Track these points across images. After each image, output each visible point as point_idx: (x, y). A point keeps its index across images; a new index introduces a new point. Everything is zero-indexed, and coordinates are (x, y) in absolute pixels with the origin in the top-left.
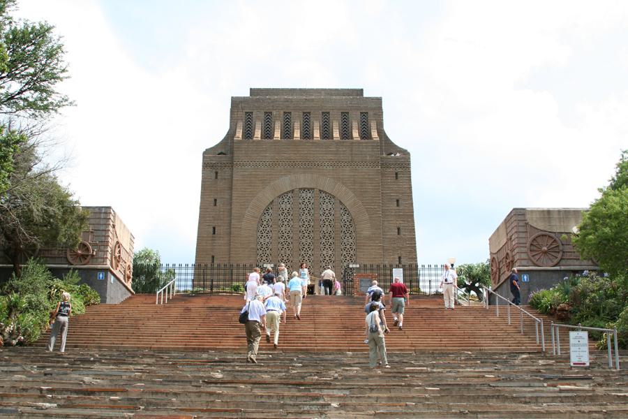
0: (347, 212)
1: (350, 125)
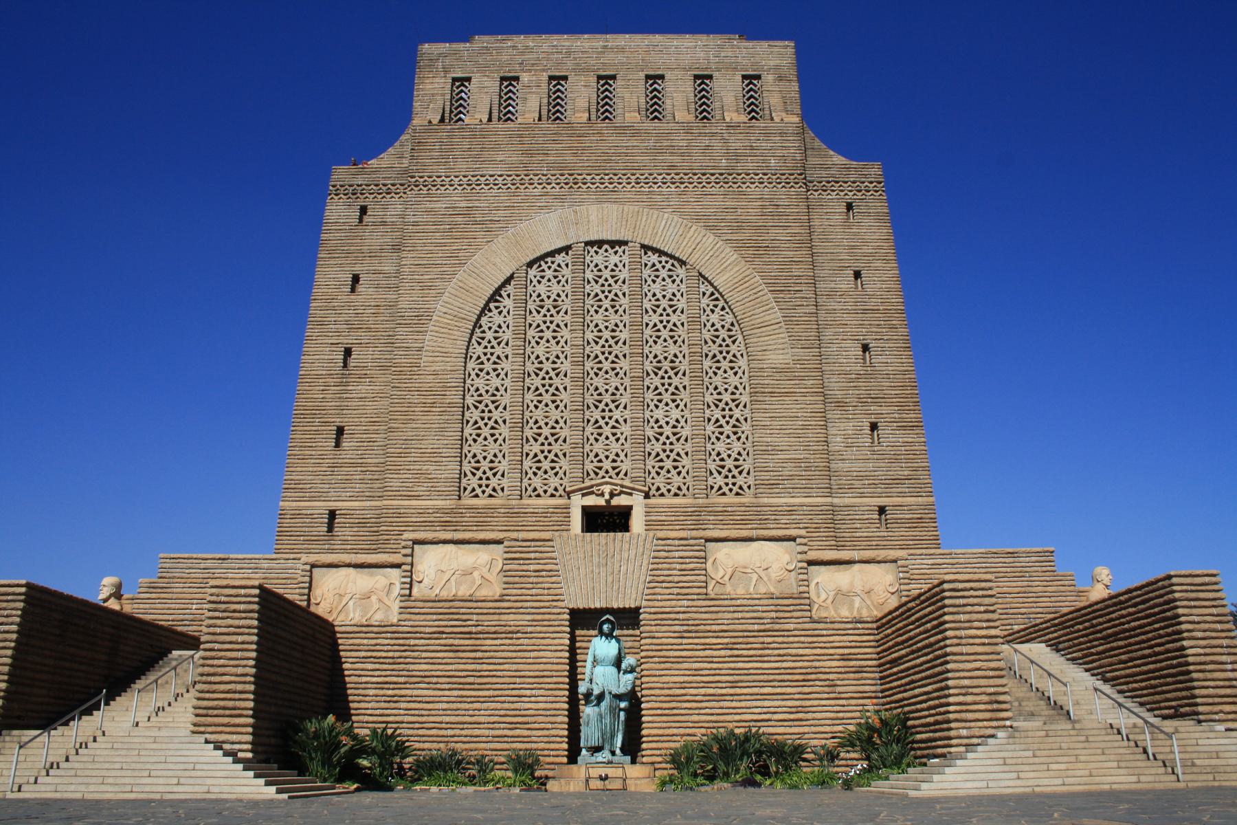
0: (721, 303)
1: (717, 105)
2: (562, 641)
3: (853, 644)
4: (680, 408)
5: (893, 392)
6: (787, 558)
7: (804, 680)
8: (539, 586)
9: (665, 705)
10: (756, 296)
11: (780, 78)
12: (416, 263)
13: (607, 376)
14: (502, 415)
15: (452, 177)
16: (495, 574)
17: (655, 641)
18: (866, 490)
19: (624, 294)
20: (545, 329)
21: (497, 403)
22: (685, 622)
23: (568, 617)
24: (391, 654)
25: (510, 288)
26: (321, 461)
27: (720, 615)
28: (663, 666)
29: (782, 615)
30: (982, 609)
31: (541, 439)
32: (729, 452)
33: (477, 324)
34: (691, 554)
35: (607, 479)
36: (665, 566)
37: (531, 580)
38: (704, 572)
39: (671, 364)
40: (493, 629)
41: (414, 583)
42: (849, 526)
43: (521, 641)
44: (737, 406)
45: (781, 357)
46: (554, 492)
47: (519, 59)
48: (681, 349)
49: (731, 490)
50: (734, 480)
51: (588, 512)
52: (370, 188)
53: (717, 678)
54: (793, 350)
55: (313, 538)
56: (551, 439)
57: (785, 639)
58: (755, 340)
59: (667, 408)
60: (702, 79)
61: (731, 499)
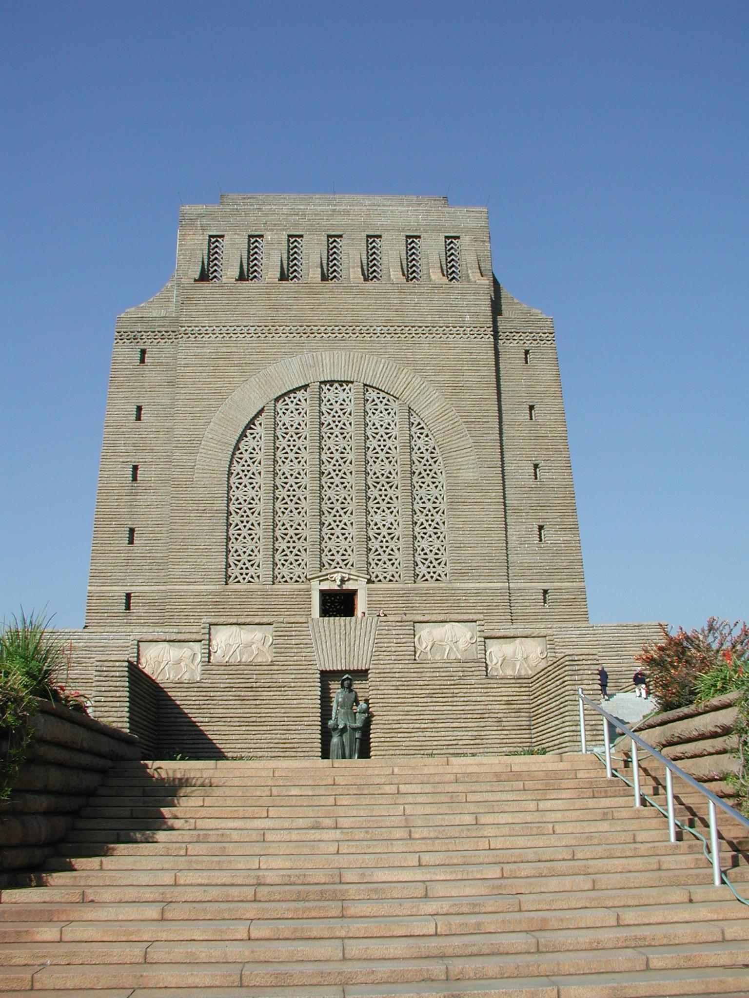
2: (315, 693)
3: (515, 693)
4: (393, 514)
5: (557, 502)
6: (469, 634)
7: (480, 718)
8: (299, 654)
9: (386, 735)
10: (453, 426)
11: (476, 240)
12: (187, 397)
13: (338, 489)
14: (257, 519)
15: (214, 327)
16: (267, 647)
17: (379, 692)
18: (534, 577)
19: (350, 424)
20: (289, 451)
21: (253, 510)
22: (399, 679)
23: (319, 676)
24: (197, 702)
25: (261, 419)
26: (118, 555)
27: (424, 674)
28: (385, 709)
29: (466, 673)
30: (590, 672)
31: (287, 538)
32: (431, 548)
33: (237, 448)
34: (404, 632)
35: (338, 569)
36: (386, 640)
37: (293, 650)
38: (413, 644)
39: (387, 480)
40: (268, 685)
41: (212, 654)
42: (521, 605)
43: (287, 693)
44: (437, 512)
45: (471, 474)
46: (298, 579)
47: (264, 220)
48: (394, 468)
49: (432, 577)
50: (434, 570)
51: (325, 595)
52: (148, 334)
53: (422, 717)
54: (481, 469)
55: (114, 615)
56: (295, 538)
57: (468, 691)
58: (452, 461)
59: (384, 514)
60: (411, 239)
61: (432, 584)
